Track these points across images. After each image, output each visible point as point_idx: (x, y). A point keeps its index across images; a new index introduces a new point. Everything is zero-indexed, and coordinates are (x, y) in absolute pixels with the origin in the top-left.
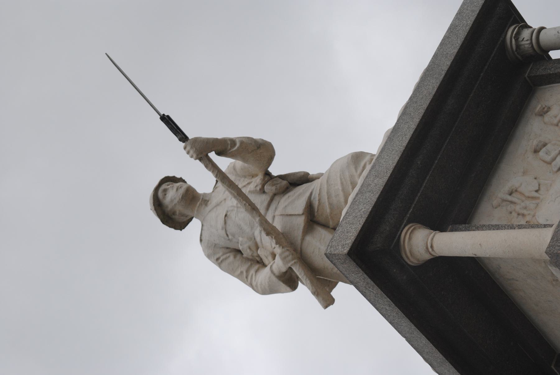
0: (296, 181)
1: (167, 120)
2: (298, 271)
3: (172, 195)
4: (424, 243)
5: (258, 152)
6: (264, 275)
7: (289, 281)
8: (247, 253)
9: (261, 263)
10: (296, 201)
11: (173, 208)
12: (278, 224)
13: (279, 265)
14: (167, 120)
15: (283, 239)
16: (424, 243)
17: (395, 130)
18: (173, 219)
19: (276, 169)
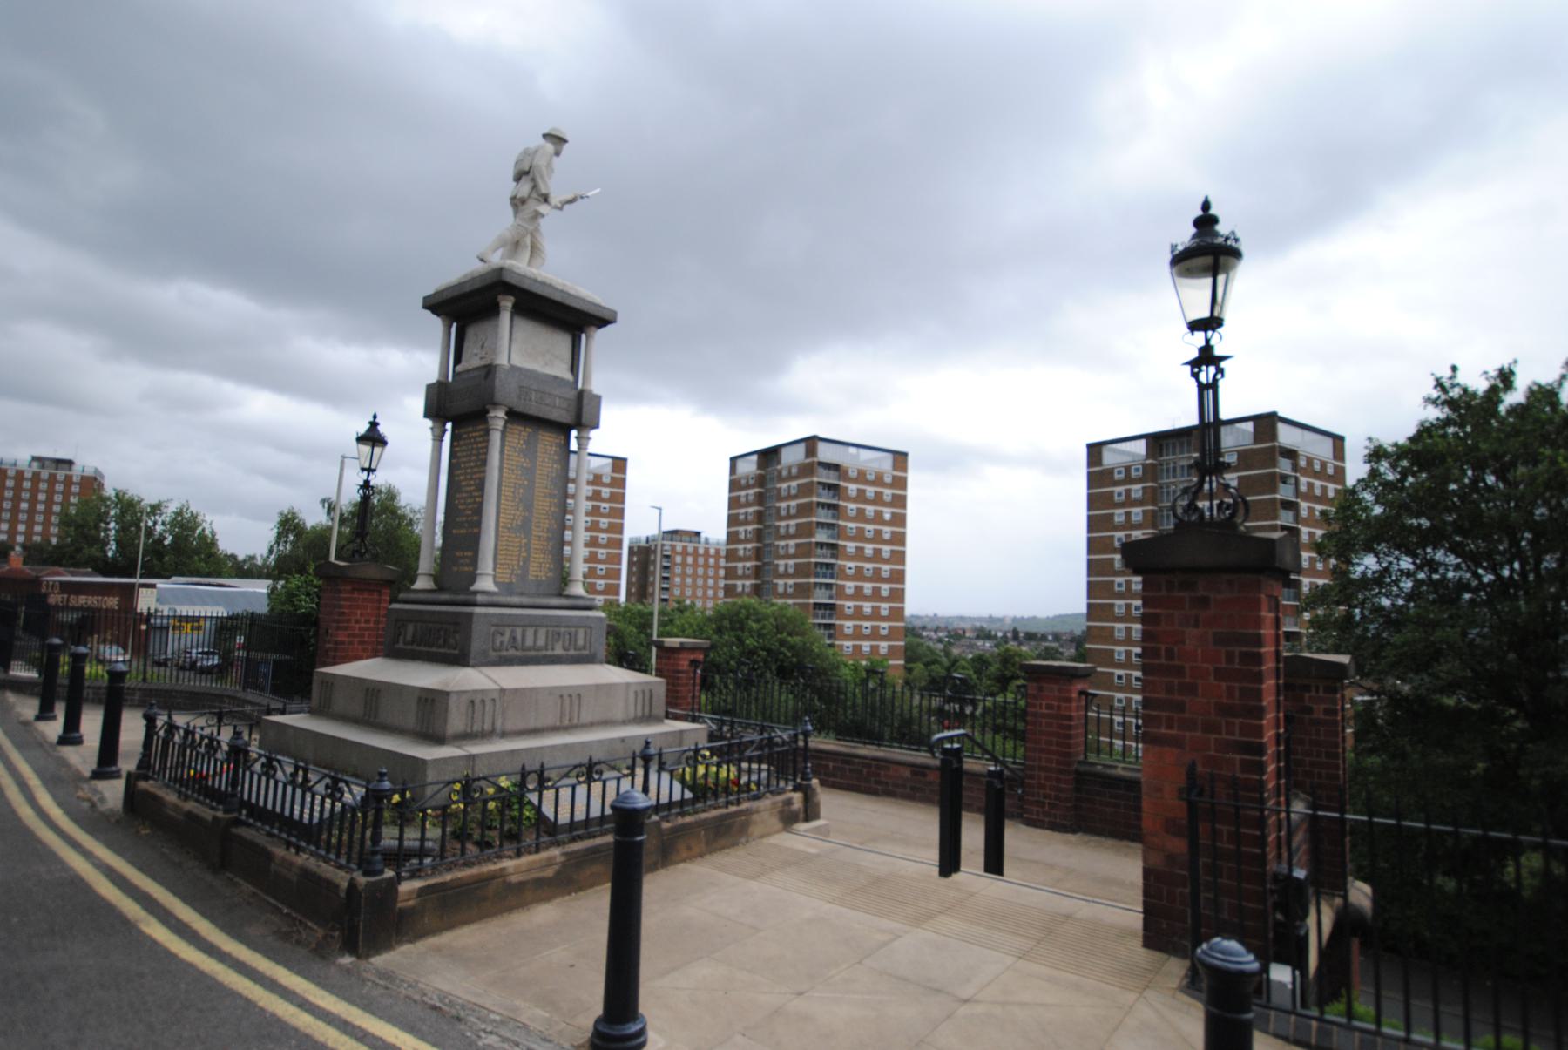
4: (507, 303)
16: (507, 303)
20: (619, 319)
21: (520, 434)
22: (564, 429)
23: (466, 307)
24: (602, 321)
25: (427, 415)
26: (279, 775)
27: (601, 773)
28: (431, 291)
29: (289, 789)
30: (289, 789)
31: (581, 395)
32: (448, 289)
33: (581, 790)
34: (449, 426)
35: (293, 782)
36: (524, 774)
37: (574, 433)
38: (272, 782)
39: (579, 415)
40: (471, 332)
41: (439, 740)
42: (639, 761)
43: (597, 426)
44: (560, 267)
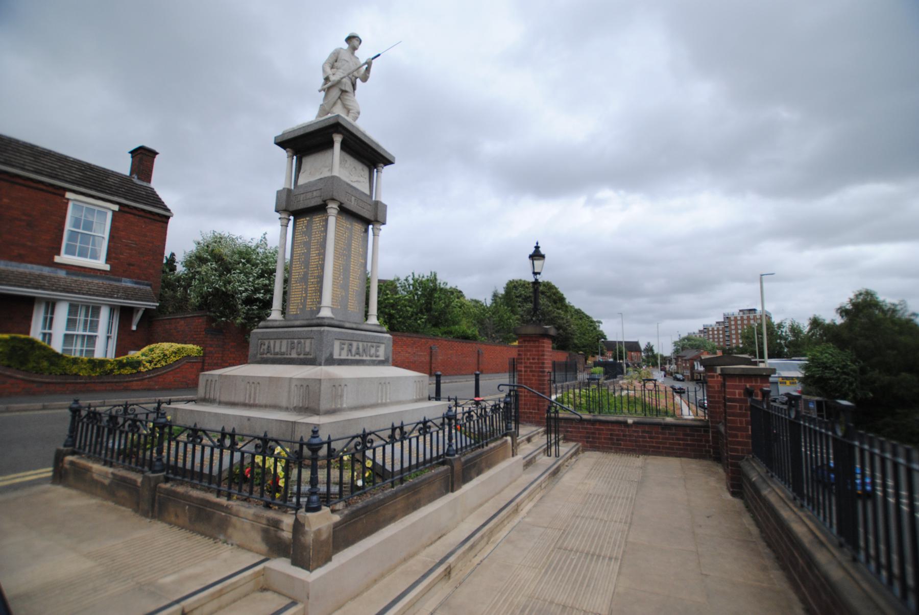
0: (354, 86)
1: (379, 55)
2: (329, 84)
3: (355, 42)
4: (338, 139)
5: (365, 79)
6: (329, 71)
7: (327, 79)
8: (336, 64)
9: (332, 67)
10: (349, 88)
11: (352, 40)
12: (344, 80)
13: (332, 78)
14: (379, 55)
15: (339, 82)
16: (338, 139)
17: (365, 136)
18: (350, 39)
19: (358, 81)
20: (396, 161)
21: (346, 223)
22: (366, 222)
23: (303, 145)
24: (388, 162)
25: (277, 211)
26: (206, 441)
27: (430, 427)
28: (280, 133)
29: (217, 451)
30: (217, 451)
31: (377, 203)
32: (294, 131)
33: (421, 438)
34: (292, 218)
35: (221, 447)
36: (394, 429)
37: (371, 227)
38: (198, 448)
39: (376, 215)
40: (304, 160)
41: (316, 412)
42: (446, 421)
43: (384, 224)
44: (369, 124)
